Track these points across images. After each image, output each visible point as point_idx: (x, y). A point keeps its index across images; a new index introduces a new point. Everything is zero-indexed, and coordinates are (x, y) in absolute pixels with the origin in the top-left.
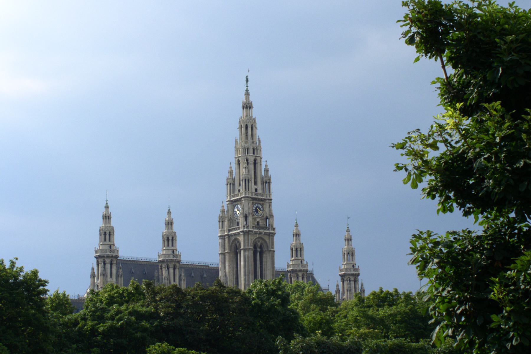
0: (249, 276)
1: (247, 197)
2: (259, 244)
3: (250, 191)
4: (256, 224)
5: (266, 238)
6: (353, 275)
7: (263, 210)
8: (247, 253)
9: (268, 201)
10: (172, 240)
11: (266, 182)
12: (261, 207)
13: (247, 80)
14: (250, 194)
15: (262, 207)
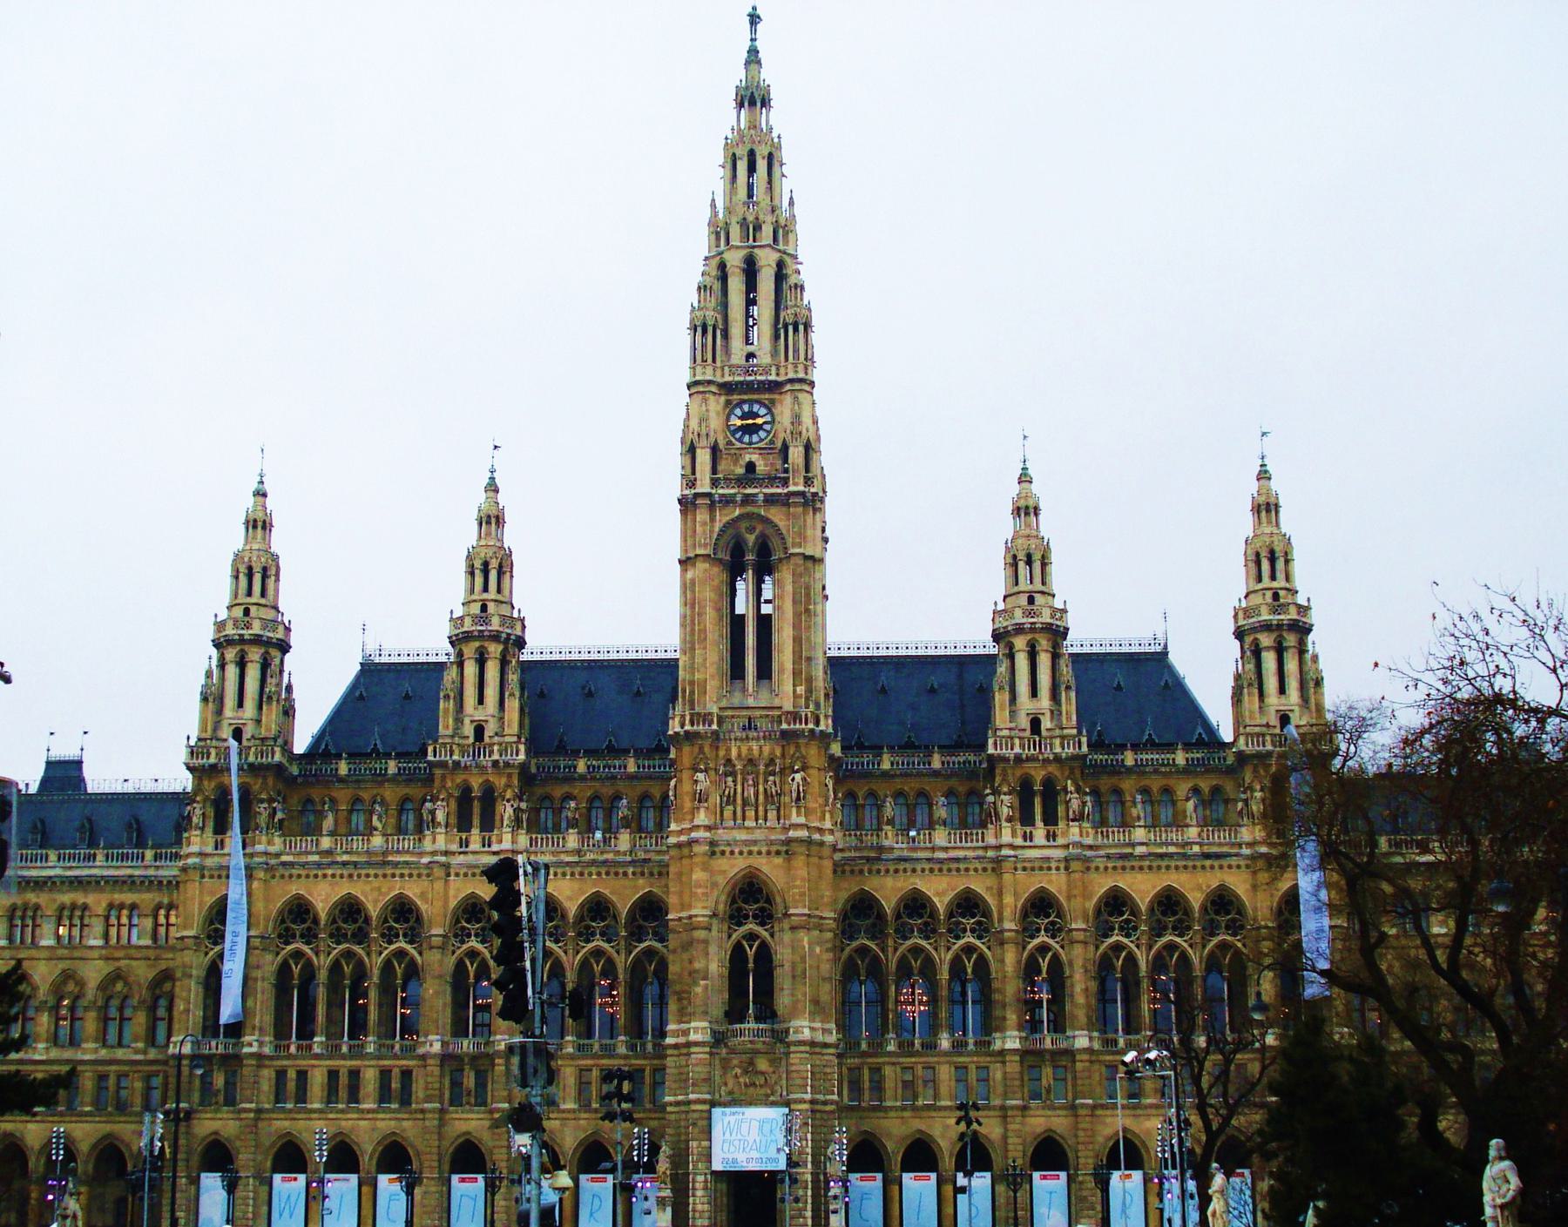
0: (693, 649)
1: (696, 383)
2: (751, 539)
3: (718, 364)
4: (741, 471)
5: (776, 515)
6: (1267, 627)
7: (773, 422)
8: (689, 575)
9: (788, 387)
10: (500, 574)
11: (786, 326)
12: (763, 411)
13: (754, 19)
14: (719, 373)
15: (770, 412)
